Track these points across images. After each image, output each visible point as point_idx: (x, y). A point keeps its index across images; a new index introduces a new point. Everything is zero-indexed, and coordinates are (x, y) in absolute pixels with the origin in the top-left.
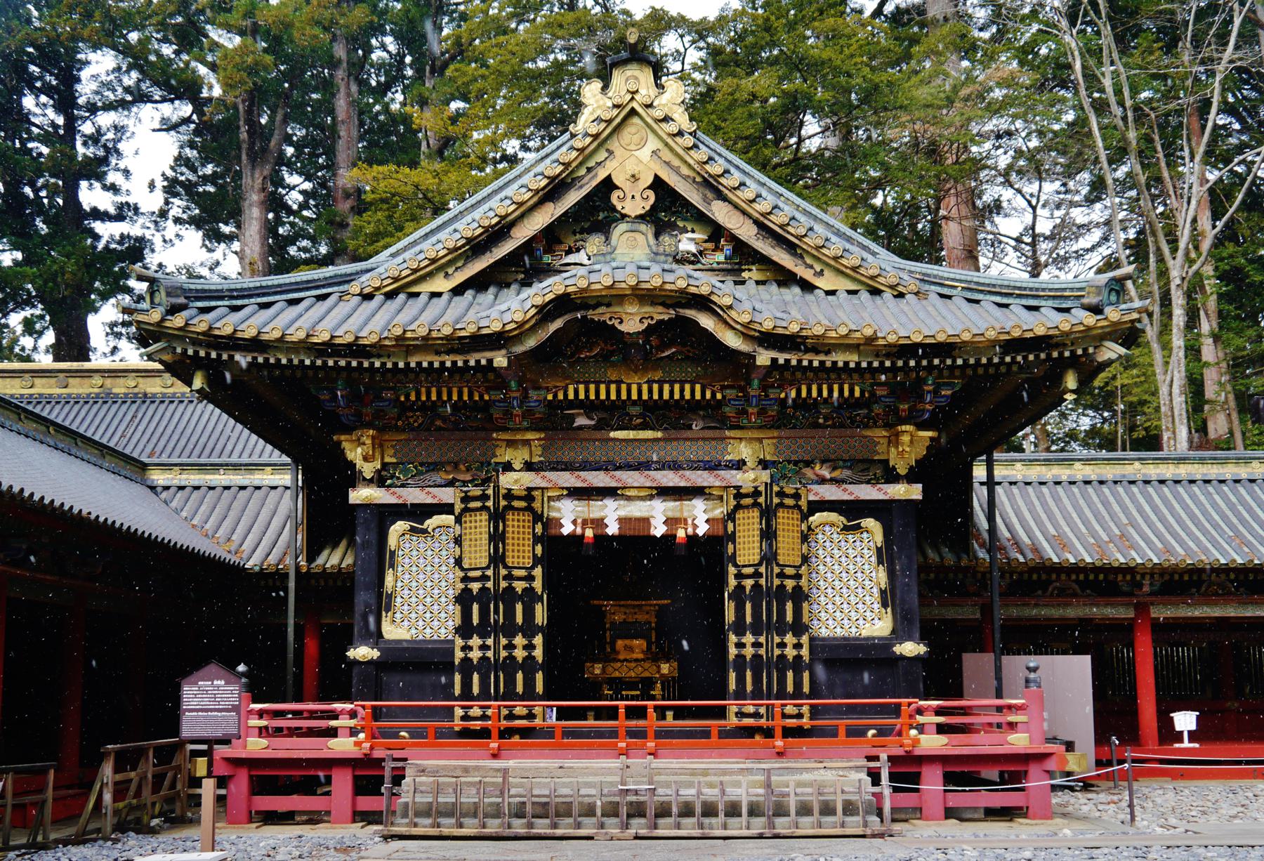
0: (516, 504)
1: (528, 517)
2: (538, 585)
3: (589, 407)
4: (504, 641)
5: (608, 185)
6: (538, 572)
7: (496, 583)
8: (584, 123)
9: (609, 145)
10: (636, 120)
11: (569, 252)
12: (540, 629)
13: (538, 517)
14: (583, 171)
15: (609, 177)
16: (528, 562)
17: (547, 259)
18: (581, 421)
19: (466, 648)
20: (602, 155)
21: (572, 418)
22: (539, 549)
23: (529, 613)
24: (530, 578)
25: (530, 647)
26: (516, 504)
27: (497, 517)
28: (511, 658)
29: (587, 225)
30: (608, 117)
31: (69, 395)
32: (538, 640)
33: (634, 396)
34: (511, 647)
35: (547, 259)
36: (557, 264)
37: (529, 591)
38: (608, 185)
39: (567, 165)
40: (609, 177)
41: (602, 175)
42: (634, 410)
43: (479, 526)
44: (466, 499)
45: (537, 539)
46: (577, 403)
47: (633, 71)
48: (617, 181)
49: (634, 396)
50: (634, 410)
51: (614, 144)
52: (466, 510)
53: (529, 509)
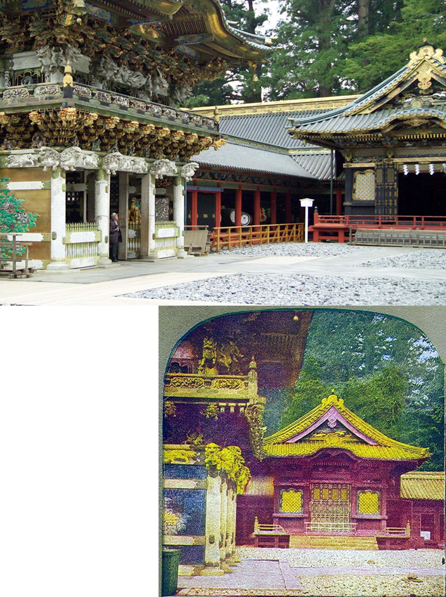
0: (390, 166)
1: (393, 170)
2: (395, 187)
3: (410, 141)
4: (387, 201)
5: (417, 81)
6: (395, 184)
7: (385, 187)
8: (410, 65)
9: (418, 70)
10: (425, 63)
11: (406, 99)
12: (396, 198)
13: (395, 170)
14: (409, 78)
15: (417, 79)
16: (393, 181)
17: (400, 101)
18: (408, 144)
19: (378, 202)
20: (415, 73)
21: (405, 144)
22: (396, 178)
23: (393, 194)
24: (394, 185)
25: (393, 202)
26: (390, 166)
27: (385, 170)
28: (389, 205)
29: (412, 91)
30: (417, 63)
31: (257, 115)
32: (395, 201)
33: (425, 137)
34: (388, 202)
35: (400, 101)
36: (403, 102)
37: (393, 188)
38: (417, 81)
39: (404, 78)
40: (417, 79)
41: (415, 79)
42: (424, 141)
43: (380, 172)
44: (377, 165)
45: (395, 175)
46: (408, 140)
47: (426, 48)
48: (419, 80)
49: (425, 137)
50: (424, 141)
51: (418, 70)
52: (377, 168)
53: (393, 168)
